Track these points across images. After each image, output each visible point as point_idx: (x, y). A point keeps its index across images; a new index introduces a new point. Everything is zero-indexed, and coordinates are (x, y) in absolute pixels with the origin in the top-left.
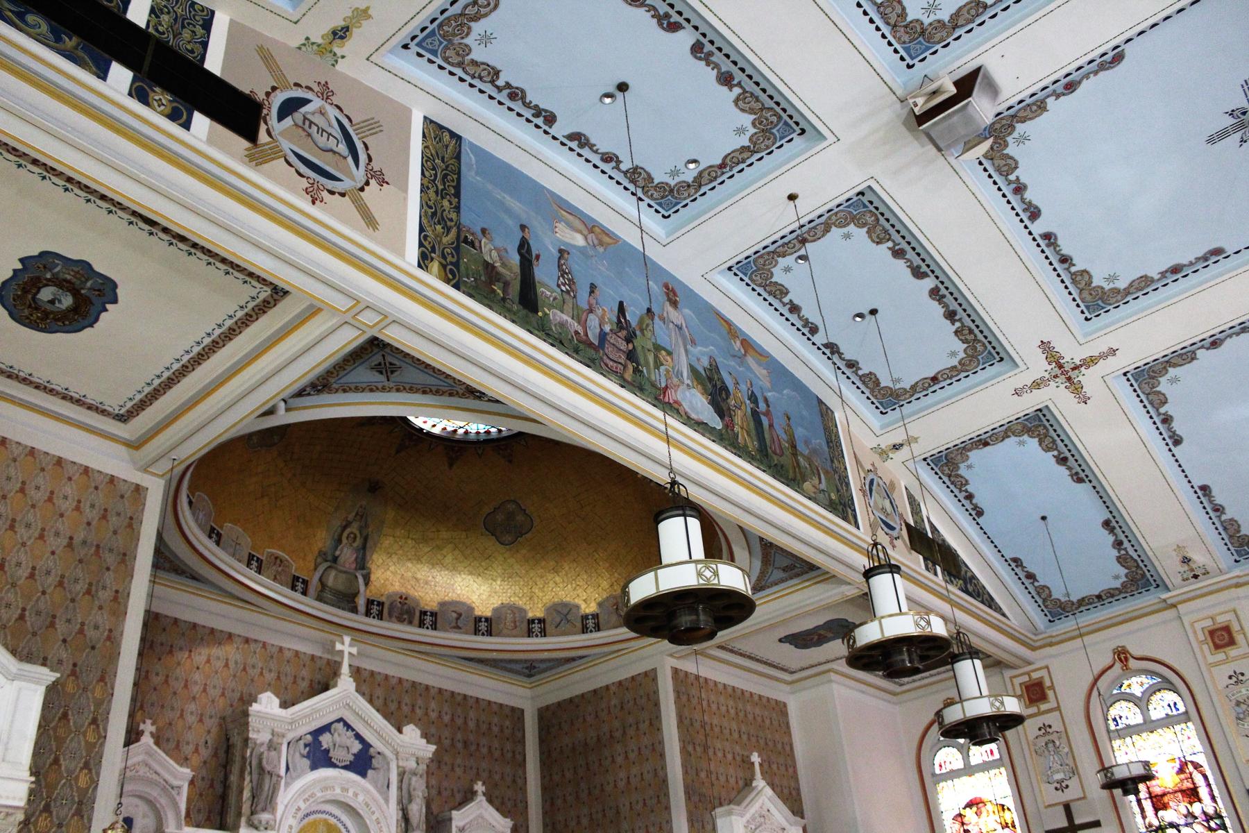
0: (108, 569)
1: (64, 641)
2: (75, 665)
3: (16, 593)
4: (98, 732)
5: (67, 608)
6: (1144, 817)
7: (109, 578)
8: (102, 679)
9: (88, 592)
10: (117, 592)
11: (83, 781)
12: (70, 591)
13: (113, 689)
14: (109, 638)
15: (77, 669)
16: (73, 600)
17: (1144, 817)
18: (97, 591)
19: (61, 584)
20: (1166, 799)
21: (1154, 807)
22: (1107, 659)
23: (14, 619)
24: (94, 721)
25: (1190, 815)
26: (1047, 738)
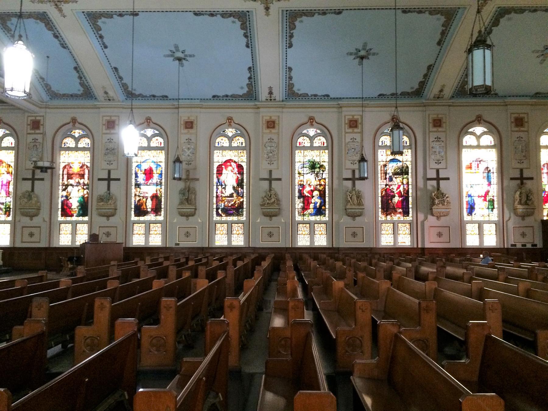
6: (63, 180)
17: (63, 180)
20: (72, 176)
21: (68, 177)
22: (68, 120)
25: (79, 183)
26: (35, 143)
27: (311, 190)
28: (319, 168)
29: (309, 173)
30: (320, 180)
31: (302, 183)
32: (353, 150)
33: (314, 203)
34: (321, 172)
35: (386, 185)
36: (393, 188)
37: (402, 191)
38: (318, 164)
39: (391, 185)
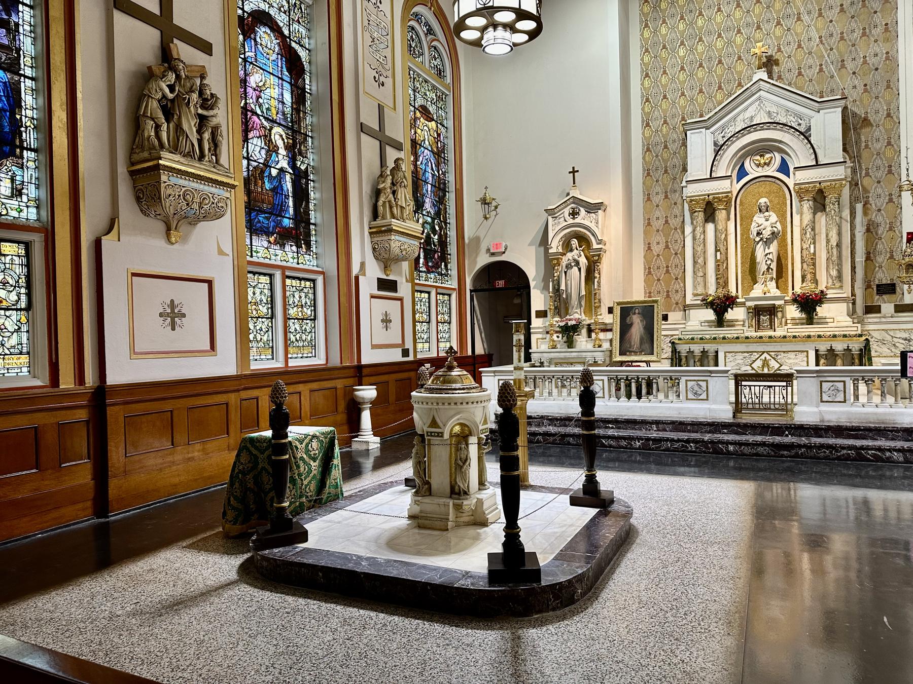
0: (875, 12)
1: (854, 73)
2: (865, 85)
3: (813, 57)
4: (894, 122)
5: (851, 51)
7: (878, 18)
8: (888, 87)
9: (864, 34)
10: (886, 24)
11: (889, 153)
12: (850, 40)
13: (898, 90)
14: (887, 58)
15: (868, 87)
16: (853, 45)
18: (870, 31)
19: (842, 38)
23: (816, 74)
24: (889, 115)
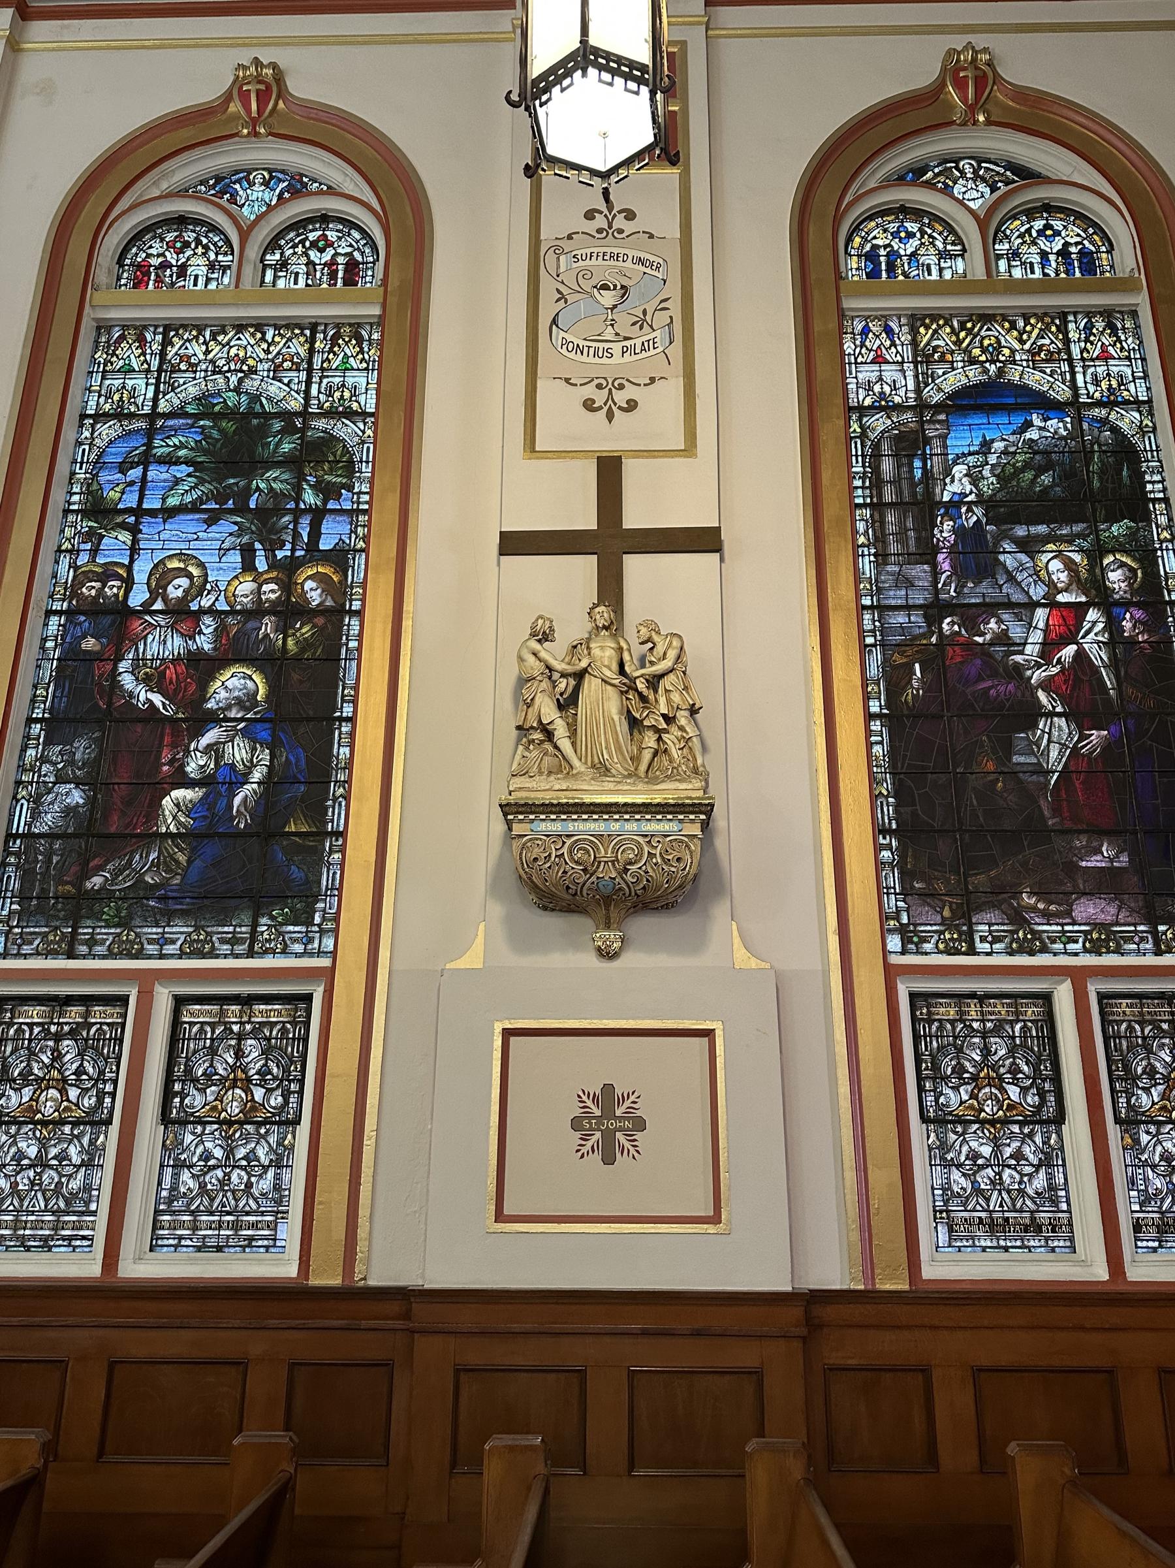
27: (194, 659)
28: (293, 463)
29: (194, 508)
30: (287, 571)
31: (113, 588)
32: (608, 298)
33: (204, 781)
34: (310, 497)
35: (935, 610)
36: (1003, 638)
37: (1098, 656)
38: (288, 430)
39: (991, 608)
